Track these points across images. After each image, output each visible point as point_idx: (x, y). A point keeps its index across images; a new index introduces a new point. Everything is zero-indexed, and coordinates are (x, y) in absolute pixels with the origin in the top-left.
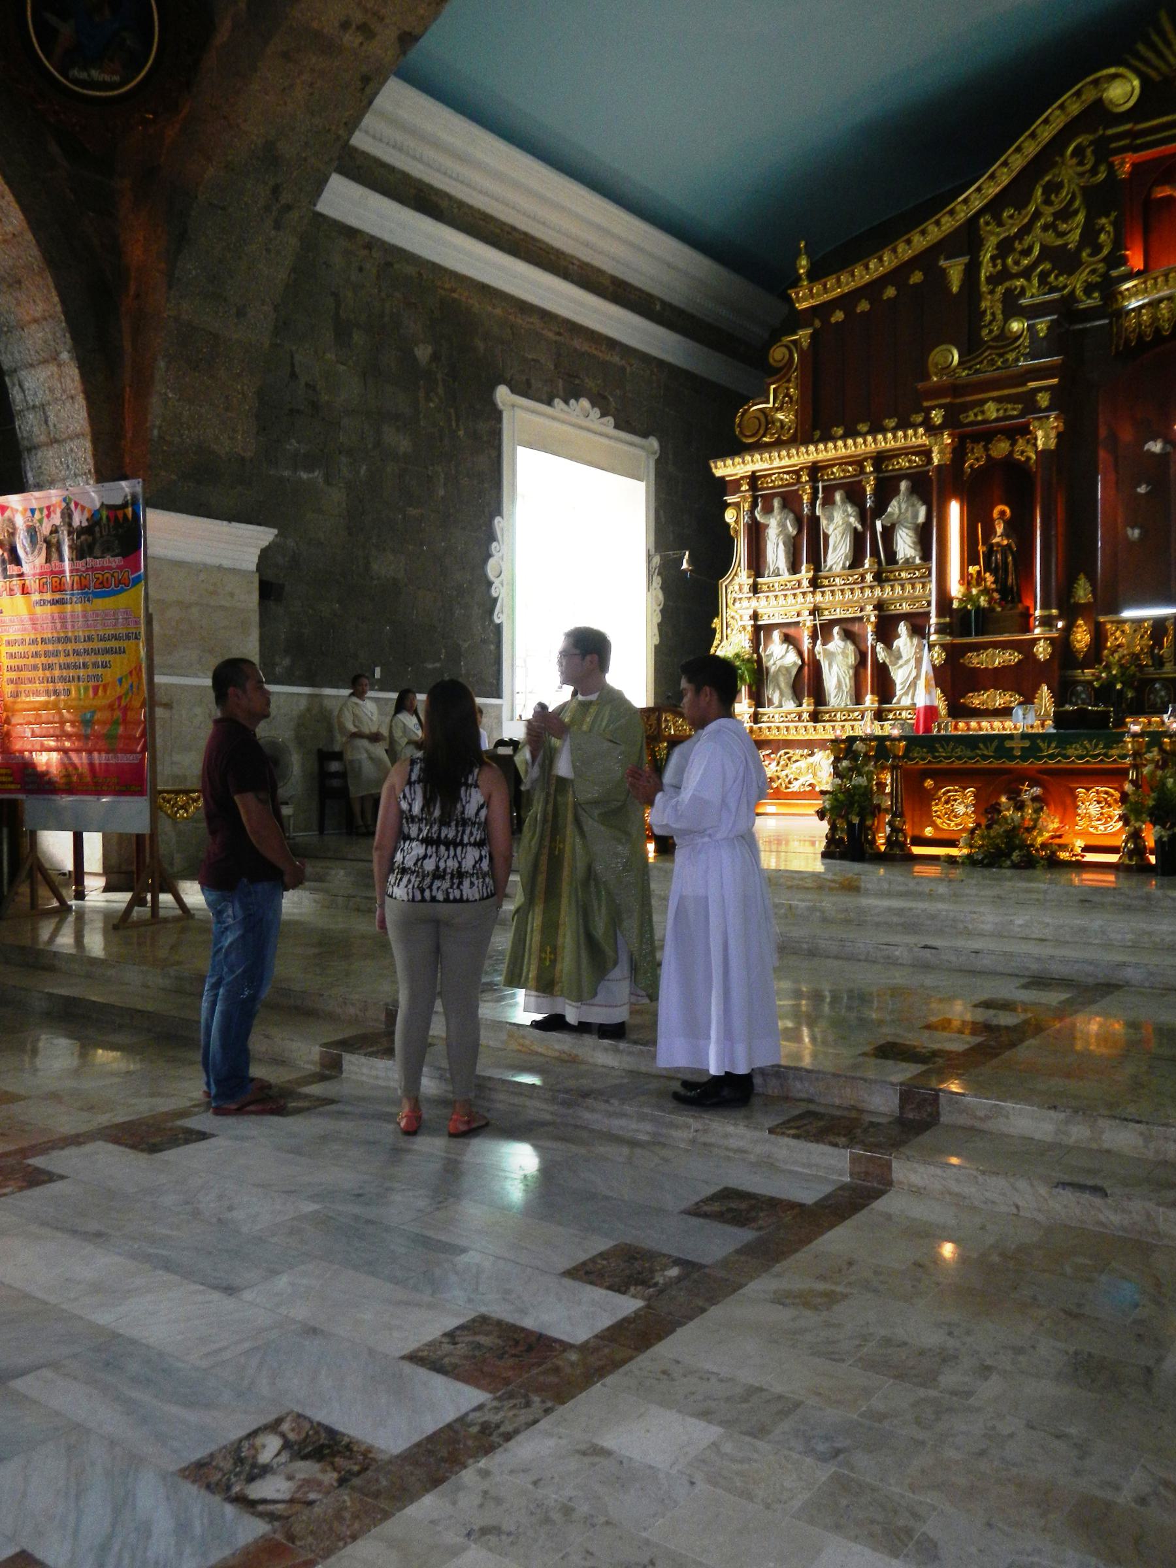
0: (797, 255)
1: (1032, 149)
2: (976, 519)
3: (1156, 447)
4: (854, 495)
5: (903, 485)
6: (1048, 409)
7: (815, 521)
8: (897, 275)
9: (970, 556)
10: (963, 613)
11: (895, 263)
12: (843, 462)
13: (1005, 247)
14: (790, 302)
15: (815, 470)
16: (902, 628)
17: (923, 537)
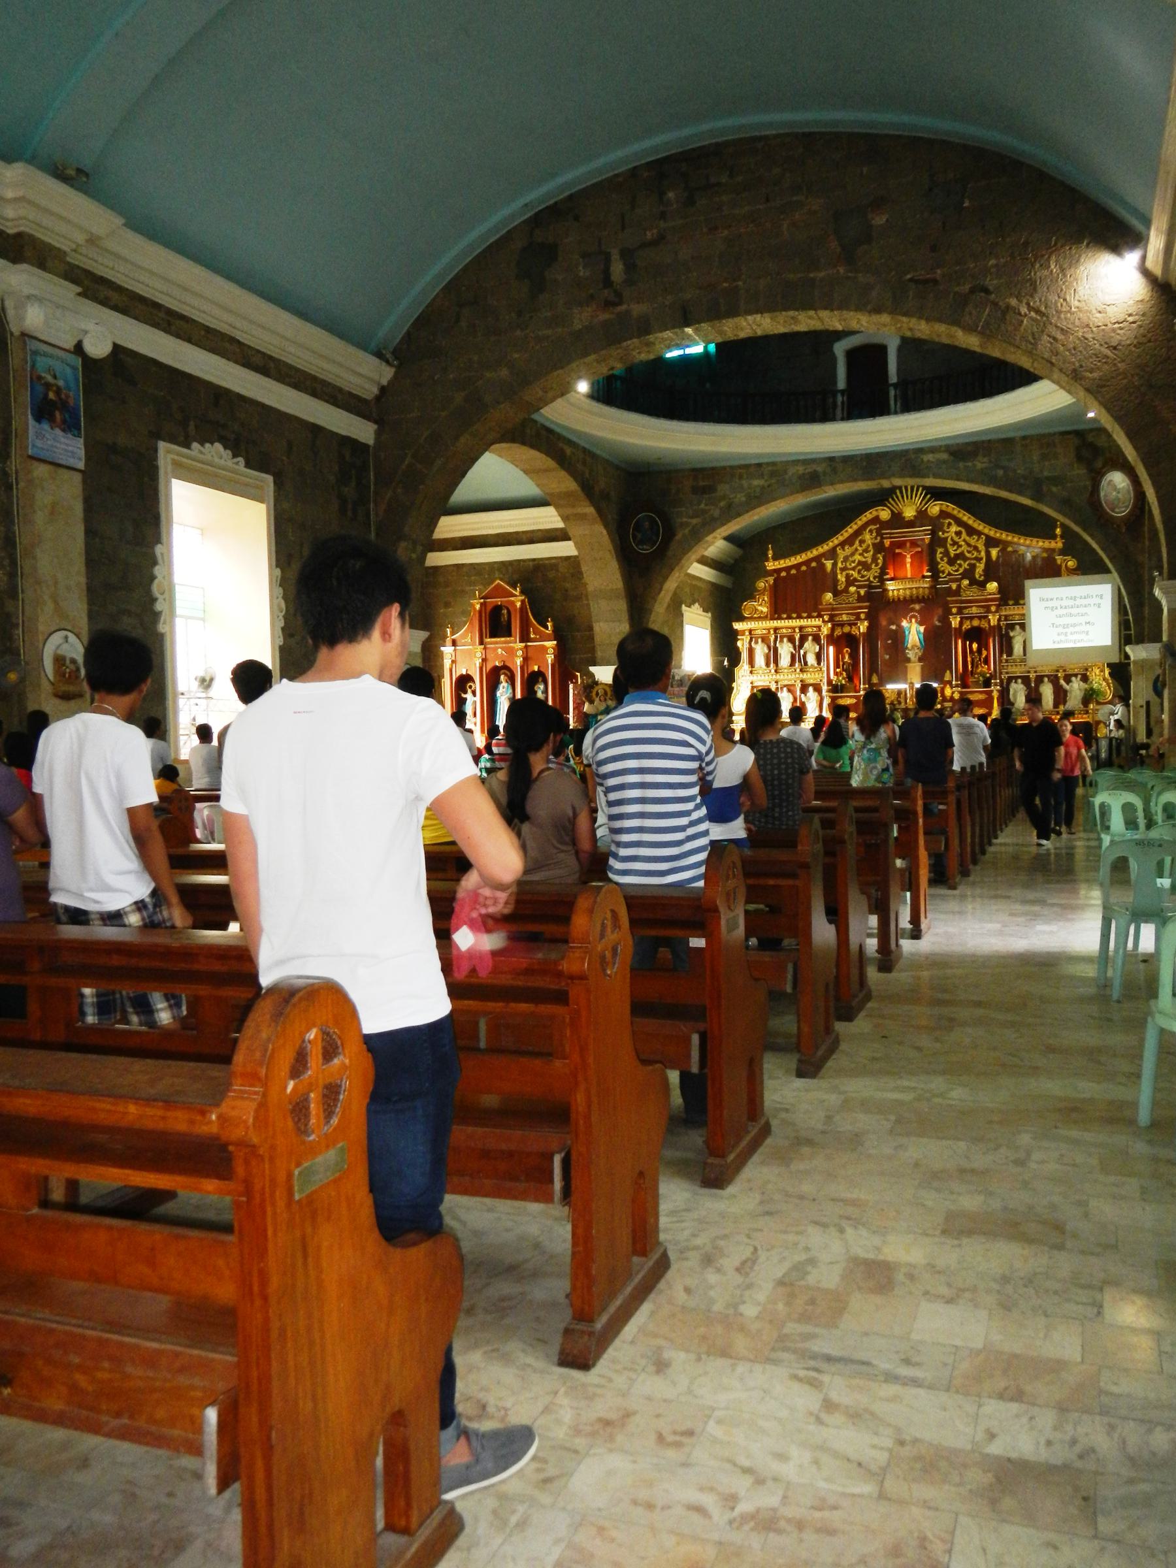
0: (768, 549)
1: (855, 527)
2: (838, 653)
3: (894, 627)
4: (791, 640)
5: (810, 638)
6: (865, 619)
7: (776, 650)
8: (807, 563)
9: (837, 665)
10: (836, 686)
11: (806, 558)
12: (787, 628)
13: (846, 559)
14: (765, 567)
15: (776, 629)
16: (811, 689)
17: (819, 657)
